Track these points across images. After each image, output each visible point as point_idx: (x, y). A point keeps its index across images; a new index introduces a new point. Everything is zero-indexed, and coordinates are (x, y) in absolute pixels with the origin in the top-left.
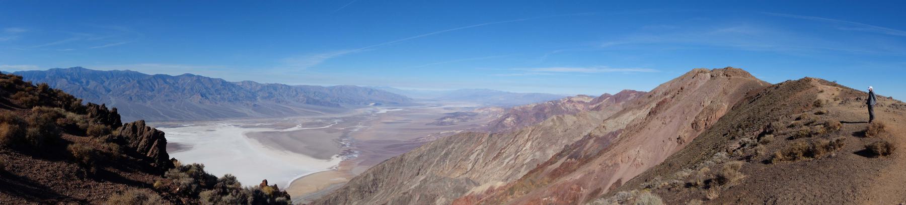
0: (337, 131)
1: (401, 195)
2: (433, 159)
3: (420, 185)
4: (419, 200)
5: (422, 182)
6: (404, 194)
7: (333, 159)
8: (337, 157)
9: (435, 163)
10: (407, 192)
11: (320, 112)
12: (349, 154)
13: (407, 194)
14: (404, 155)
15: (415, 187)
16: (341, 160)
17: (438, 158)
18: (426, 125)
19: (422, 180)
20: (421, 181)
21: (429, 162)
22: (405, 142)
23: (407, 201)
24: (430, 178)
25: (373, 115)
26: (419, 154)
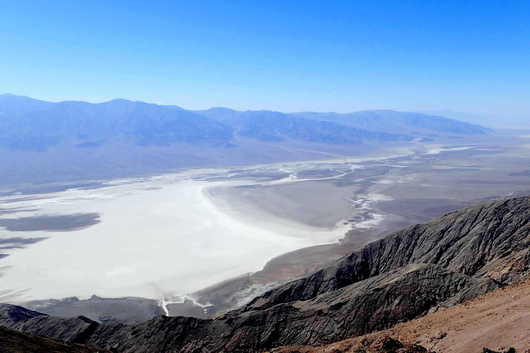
0: (350, 184)
1: (372, 292)
2: (467, 236)
3: (404, 280)
4: (399, 304)
5: (410, 275)
6: (378, 290)
7: (337, 227)
8: (345, 224)
9: (469, 245)
10: (382, 289)
11: (329, 154)
12: (365, 220)
13: (381, 292)
14: (417, 227)
15: (397, 282)
16: (350, 229)
17: (475, 238)
18: (513, 174)
19: (411, 273)
20: (409, 273)
21: (459, 242)
22: (463, 203)
23: (378, 303)
24: (426, 270)
25: (416, 157)
26: (443, 227)
